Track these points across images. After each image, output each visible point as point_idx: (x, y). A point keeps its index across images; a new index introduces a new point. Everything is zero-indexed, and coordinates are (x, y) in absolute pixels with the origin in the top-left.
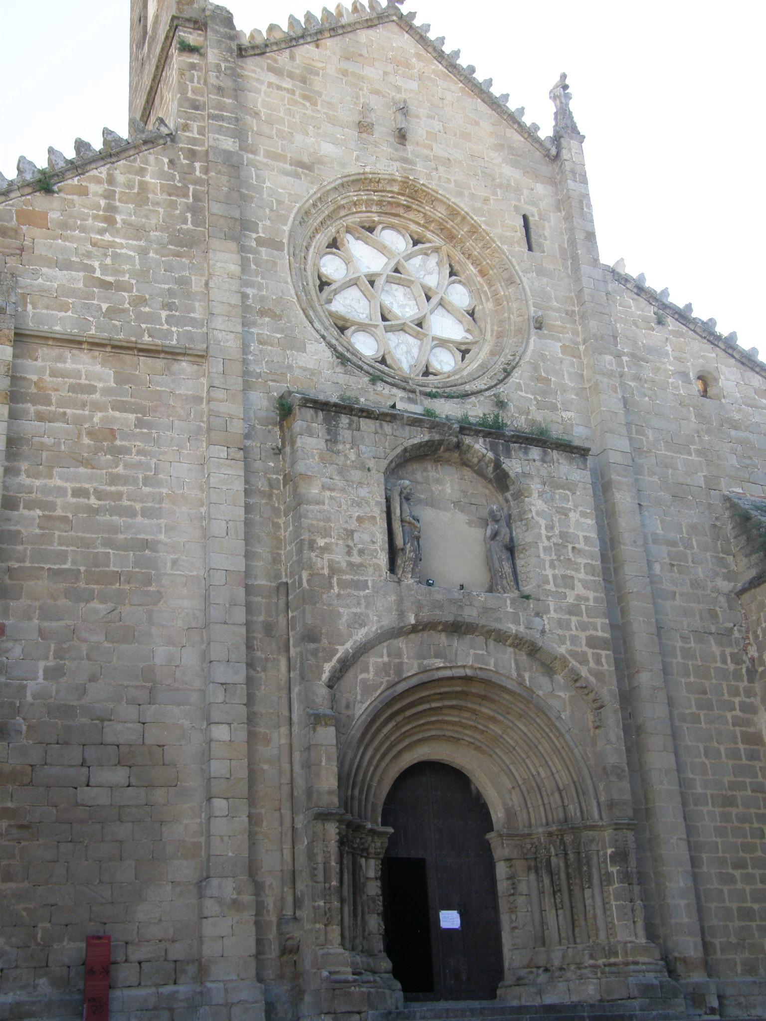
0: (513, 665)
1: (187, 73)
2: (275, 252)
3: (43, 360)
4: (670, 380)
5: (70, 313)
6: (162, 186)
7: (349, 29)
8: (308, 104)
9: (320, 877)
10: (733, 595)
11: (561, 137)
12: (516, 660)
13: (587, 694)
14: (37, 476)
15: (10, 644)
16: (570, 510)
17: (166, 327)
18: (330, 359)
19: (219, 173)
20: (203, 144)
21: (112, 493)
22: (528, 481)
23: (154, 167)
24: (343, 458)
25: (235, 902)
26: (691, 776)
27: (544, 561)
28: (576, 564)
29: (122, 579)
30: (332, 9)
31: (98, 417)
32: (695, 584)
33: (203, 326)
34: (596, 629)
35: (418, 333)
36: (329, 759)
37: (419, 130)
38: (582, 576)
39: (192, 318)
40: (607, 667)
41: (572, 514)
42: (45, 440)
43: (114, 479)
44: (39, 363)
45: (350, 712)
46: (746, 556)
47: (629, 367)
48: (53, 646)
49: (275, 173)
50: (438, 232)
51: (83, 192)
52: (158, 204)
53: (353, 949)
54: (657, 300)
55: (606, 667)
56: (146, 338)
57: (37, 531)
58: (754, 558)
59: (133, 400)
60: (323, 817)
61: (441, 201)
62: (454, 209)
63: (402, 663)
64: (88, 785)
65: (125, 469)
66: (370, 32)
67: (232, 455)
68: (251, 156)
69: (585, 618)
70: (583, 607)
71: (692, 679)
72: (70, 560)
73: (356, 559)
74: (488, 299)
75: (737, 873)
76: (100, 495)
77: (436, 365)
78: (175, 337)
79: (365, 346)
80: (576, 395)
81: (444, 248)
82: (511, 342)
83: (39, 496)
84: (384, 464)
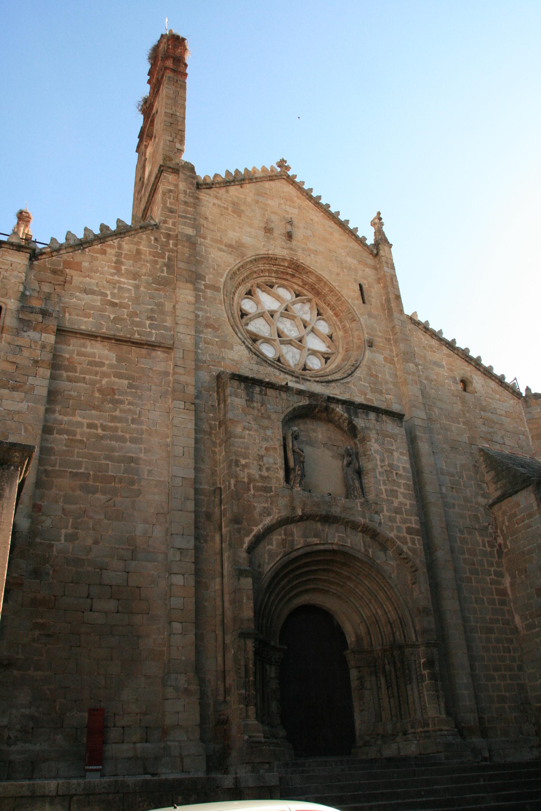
0: (362, 544)
1: (167, 194)
2: (216, 293)
3: (74, 346)
4: (446, 381)
5: (91, 319)
6: (150, 252)
7: (260, 180)
8: (235, 216)
9: (243, 674)
10: (487, 507)
11: (379, 244)
12: (363, 541)
13: (407, 563)
14: (66, 414)
15: (44, 518)
16: (394, 450)
17: (148, 330)
18: (248, 355)
19: (183, 246)
20: (174, 230)
21: (111, 427)
22: (369, 432)
23: (145, 243)
24: (256, 411)
25: (186, 690)
26: (468, 615)
27: (380, 480)
28: (398, 483)
29: (116, 480)
30: (250, 169)
31: (105, 381)
32: (466, 500)
33: (171, 330)
34: (411, 523)
35: (300, 346)
36: (248, 598)
37: (298, 234)
38: (402, 490)
39: (165, 326)
40: (419, 546)
41: (395, 453)
42: (72, 393)
43: (113, 419)
44: (71, 348)
45: (261, 570)
46: (495, 483)
47: (423, 372)
48: (71, 520)
49: (216, 250)
50: (310, 290)
51: (104, 253)
52: (147, 261)
53: (262, 723)
54: (436, 336)
55: (418, 546)
56: (137, 336)
57: (64, 448)
58: (499, 485)
59: (127, 372)
60: (244, 635)
61: (312, 273)
62: (320, 278)
63: (293, 540)
64: (91, 611)
65: (120, 413)
66: (271, 183)
67: (187, 407)
68: (202, 240)
69: (405, 516)
70: (404, 509)
71: (466, 556)
72: (84, 467)
73: (265, 473)
74: (340, 329)
75: (495, 674)
76: (104, 428)
77: (310, 365)
78: (154, 336)
79: (268, 351)
80: (394, 385)
81: (314, 300)
82: (354, 355)
83: (66, 426)
84: (282, 416)
